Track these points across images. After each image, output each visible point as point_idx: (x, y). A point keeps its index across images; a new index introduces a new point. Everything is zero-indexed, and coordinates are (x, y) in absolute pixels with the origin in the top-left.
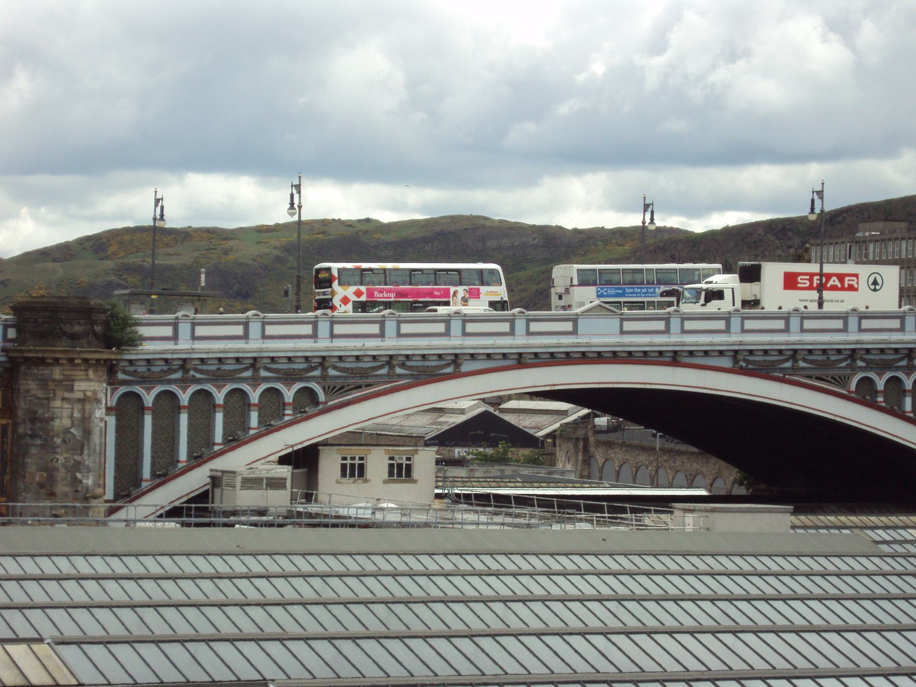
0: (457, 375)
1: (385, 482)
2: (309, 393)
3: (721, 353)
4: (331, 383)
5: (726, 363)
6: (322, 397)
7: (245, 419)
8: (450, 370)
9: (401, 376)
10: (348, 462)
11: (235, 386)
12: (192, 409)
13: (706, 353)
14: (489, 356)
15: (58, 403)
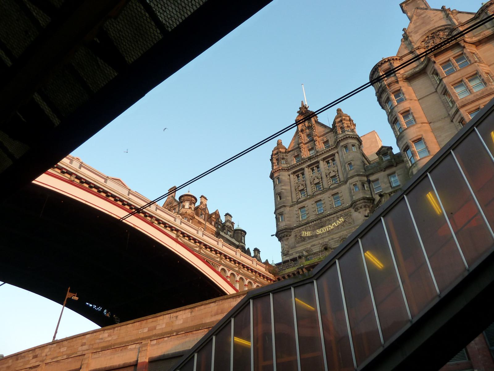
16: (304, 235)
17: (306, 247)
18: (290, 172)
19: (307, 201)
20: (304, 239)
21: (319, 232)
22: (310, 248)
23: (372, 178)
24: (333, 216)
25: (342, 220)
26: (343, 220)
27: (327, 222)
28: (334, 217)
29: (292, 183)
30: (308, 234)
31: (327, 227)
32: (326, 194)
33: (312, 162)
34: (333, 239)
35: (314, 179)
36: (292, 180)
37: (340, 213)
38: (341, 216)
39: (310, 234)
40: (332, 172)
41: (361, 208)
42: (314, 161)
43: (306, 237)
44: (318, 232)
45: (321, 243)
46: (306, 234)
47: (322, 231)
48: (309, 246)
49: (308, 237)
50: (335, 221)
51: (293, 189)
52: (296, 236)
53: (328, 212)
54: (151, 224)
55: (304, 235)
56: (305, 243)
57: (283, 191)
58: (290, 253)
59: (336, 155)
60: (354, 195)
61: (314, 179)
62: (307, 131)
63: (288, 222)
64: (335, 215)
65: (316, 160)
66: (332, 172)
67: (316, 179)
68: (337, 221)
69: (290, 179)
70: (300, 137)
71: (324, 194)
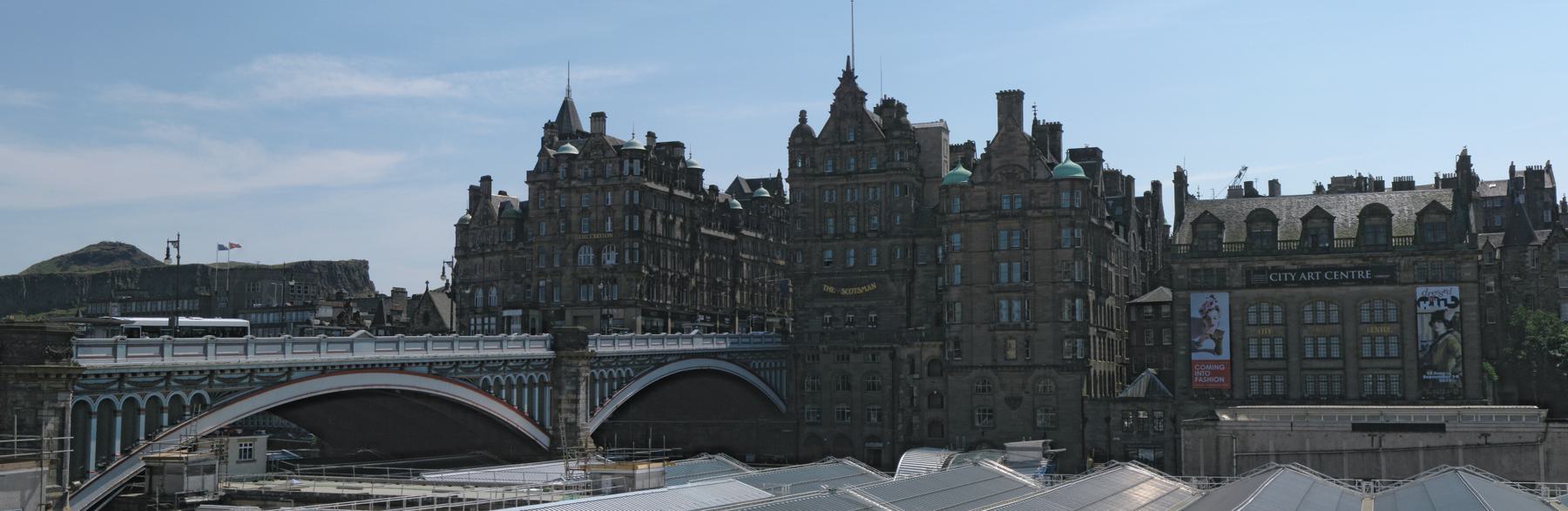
0: (289, 382)
1: (238, 462)
2: (198, 398)
3: (424, 364)
4: (215, 389)
5: (424, 369)
6: (208, 401)
7: (159, 419)
8: (284, 379)
9: (256, 384)
10: (243, 447)
11: (197, 392)
12: (100, 415)
13: (417, 364)
14: (307, 368)
15: (45, 412)
18: (817, 184)
19: (836, 243)
20: (826, 295)
21: (844, 292)
25: (874, 286)
30: (831, 289)
33: (849, 182)
34: (860, 306)
36: (817, 198)
37: (874, 276)
41: (898, 281)
48: (830, 306)
49: (831, 294)
50: (866, 284)
54: (716, 358)
58: (806, 306)
63: (807, 266)
64: (866, 277)
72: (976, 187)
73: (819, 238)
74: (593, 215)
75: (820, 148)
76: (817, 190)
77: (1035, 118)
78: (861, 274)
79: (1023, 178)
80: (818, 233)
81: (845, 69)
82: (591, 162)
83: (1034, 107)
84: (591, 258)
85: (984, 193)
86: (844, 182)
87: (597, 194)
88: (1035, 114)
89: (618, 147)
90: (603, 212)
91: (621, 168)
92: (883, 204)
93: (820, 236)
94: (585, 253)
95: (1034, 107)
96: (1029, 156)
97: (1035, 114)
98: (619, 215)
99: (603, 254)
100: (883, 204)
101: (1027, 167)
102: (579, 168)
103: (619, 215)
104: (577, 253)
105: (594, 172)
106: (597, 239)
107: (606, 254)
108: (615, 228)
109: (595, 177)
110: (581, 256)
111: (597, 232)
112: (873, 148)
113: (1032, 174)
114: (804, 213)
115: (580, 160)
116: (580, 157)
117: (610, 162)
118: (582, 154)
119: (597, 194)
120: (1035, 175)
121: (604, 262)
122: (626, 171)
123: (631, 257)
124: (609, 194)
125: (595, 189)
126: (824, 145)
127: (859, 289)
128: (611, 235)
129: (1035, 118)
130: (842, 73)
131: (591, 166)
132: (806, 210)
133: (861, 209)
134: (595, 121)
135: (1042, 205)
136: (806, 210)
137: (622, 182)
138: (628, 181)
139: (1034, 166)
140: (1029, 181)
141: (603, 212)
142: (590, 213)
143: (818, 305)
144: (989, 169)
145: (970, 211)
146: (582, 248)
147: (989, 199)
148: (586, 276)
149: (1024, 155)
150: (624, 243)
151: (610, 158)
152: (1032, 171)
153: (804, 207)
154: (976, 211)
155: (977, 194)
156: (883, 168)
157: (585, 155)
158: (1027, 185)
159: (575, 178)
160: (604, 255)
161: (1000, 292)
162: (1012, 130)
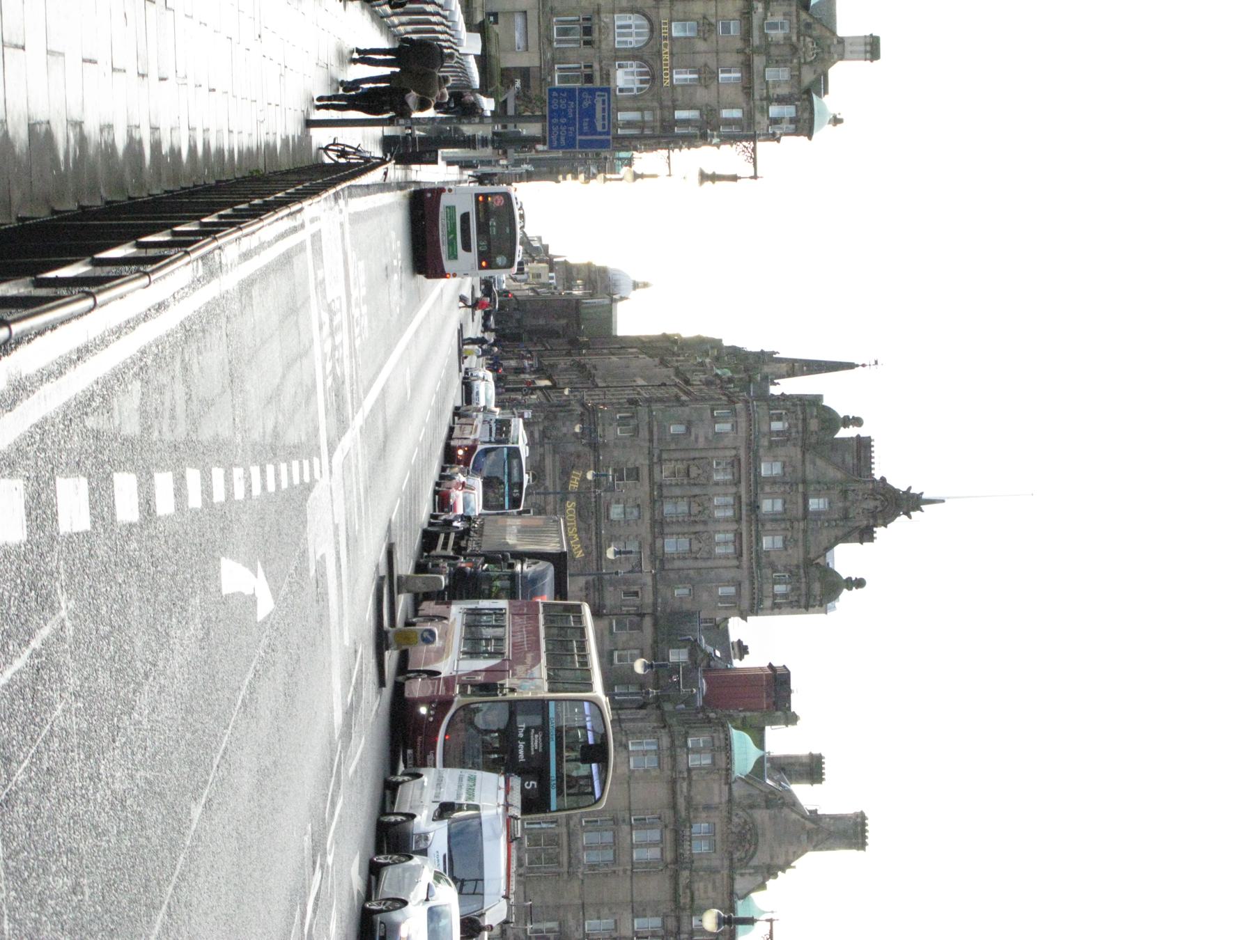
16: (575, 475)
17: (548, 477)
19: (647, 489)
20: (566, 474)
22: (544, 484)
23: (648, 622)
24: (594, 538)
26: (578, 556)
27: (582, 525)
28: (590, 539)
29: (710, 454)
31: (575, 523)
32: (649, 529)
33: (744, 507)
35: (699, 505)
36: (721, 453)
37: (594, 553)
38: (588, 554)
39: (572, 487)
40: (701, 545)
42: (744, 512)
43: (569, 478)
44: (569, 504)
45: (547, 508)
46: (574, 480)
47: (571, 512)
51: (697, 454)
52: (579, 456)
53: (603, 532)
55: (575, 475)
56: (557, 474)
57: (693, 438)
59: (735, 563)
60: (615, 590)
61: (699, 505)
62: (840, 505)
64: (594, 542)
65: (744, 517)
66: (701, 545)
67: (700, 508)
68: (579, 546)
69: (725, 448)
70: (826, 488)
71: (649, 525)
72: (726, 788)
73: (655, 460)
74: (701, 45)
75: (800, 456)
76: (733, 452)
77: (857, 366)
78: (598, 534)
79: (737, 855)
80: (665, 456)
81: (924, 496)
82: (794, 38)
83: (876, 363)
84: (629, 39)
85: (716, 800)
86: (744, 499)
87: (738, 52)
88: (864, 365)
89: (820, 85)
90: (706, 65)
91: (781, 100)
92: (709, 564)
93: (660, 459)
94: (637, 27)
95: (876, 363)
96: (769, 865)
97: (864, 365)
98: (702, 95)
99: (634, 64)
100: (709, 564)
101: (755, 862)
102: (785, 14)
103: (702, 95)
104: (638, 12)
105: (777, 45)
106: (659, 53)
107: (635, 69)
108: (679, 89)
109: (766, 48)
110: (633, 20)
111: (672, 54)
112: (796, 541)
113: (743, 871)
114: (697, 438)
115: (798, 16)
116: (804, 15)
117: (792, 76)
118: (809, 20)
119: (738, 52)
120: (742, 875)
121: (620, 66)
122: (774, 110)
123: (629, 124)
124: (739, 75)
125: (747, 51)
126: (803, 461)
127: (575, 529)
128: (667, 83)
129: (857, 366)
130: (918, 493)
131: (787, 38)
132: (701, 440)
133: (699, 528)
134: (866, 44)
135: (696, 886)
136: (701, 440)
137: (758, 103)
138: (758, 117)
139: (756, 872)
140: (732, 868)
141: (706, 65)
142: (705, 40)
143: (548, 462)
144: (752, 807)
145: (690, 784)
146: (645, 22)
147: (708, 808)
148: (596, 35)
149: (772, 858)
150: (653, 110)
151: (799, 76)
152: (747, 871)
153: (706, 438)
154: (689, 791)
155: (716, 791)
156: (764, 560)
157: (808, 26)
158: (726, 863)
159: (766, 9)
160: (633, 67)
161: (569, 835)
162: (809, 838)
